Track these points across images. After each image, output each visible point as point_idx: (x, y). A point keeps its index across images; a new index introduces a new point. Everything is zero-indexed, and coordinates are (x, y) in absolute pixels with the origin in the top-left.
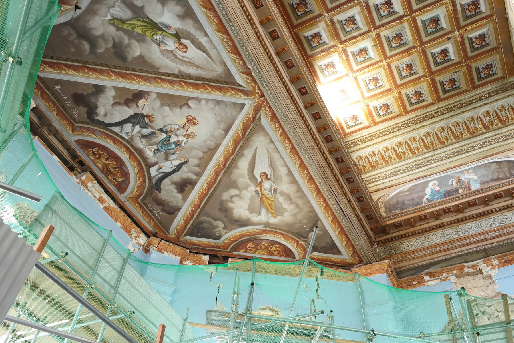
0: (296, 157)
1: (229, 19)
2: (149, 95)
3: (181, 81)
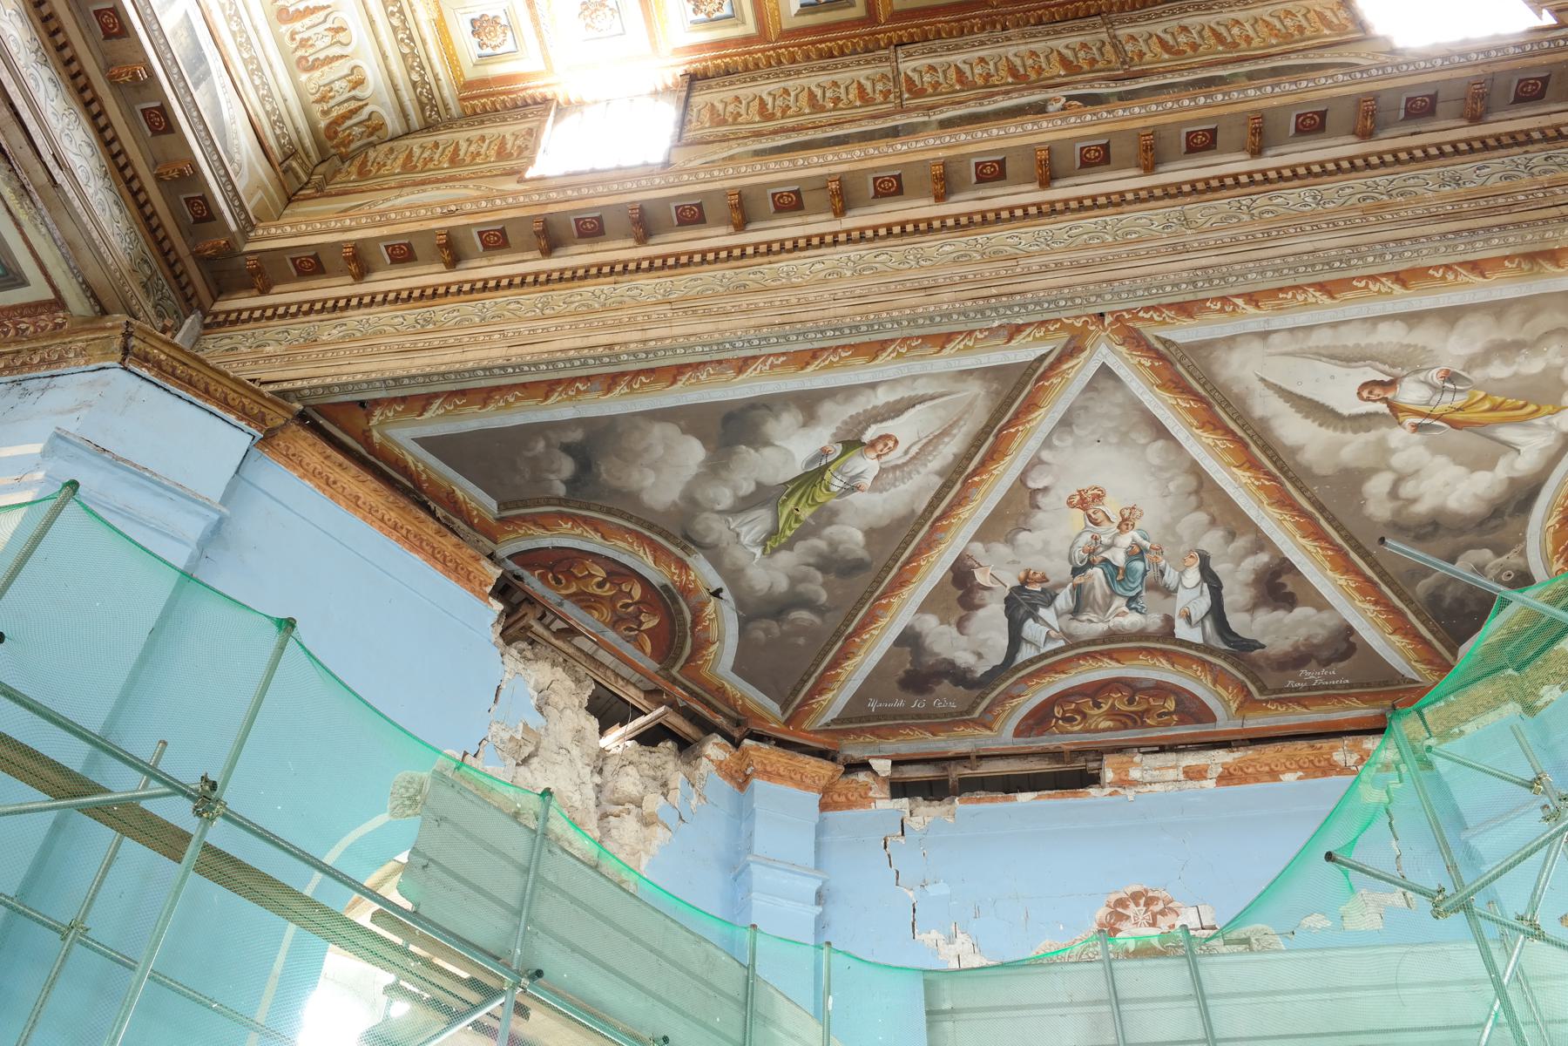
0: (1363, 284)
1: (851, 328)
2: (970, 557)
3: (965, 481)
